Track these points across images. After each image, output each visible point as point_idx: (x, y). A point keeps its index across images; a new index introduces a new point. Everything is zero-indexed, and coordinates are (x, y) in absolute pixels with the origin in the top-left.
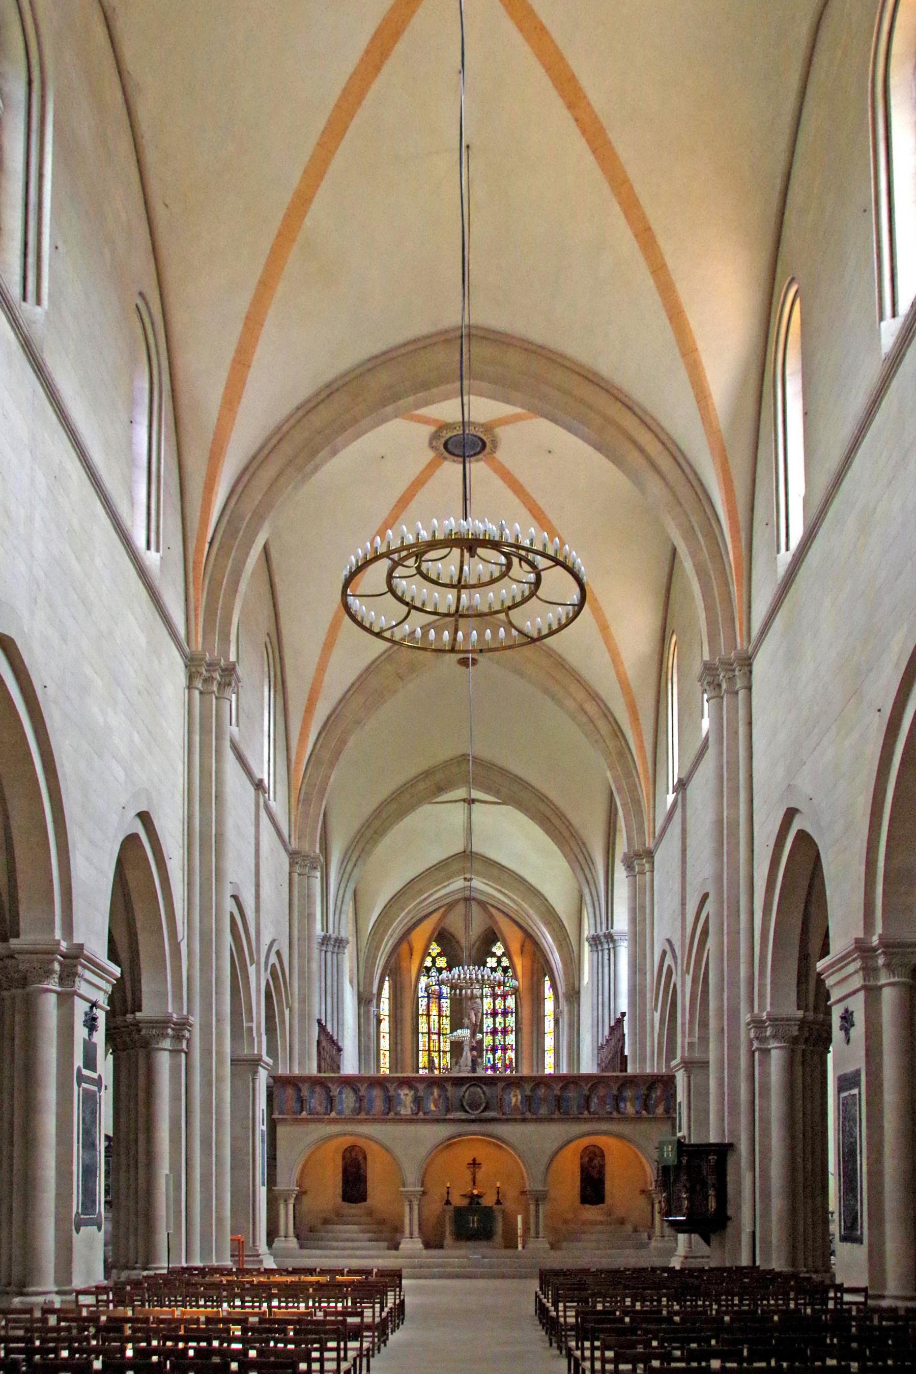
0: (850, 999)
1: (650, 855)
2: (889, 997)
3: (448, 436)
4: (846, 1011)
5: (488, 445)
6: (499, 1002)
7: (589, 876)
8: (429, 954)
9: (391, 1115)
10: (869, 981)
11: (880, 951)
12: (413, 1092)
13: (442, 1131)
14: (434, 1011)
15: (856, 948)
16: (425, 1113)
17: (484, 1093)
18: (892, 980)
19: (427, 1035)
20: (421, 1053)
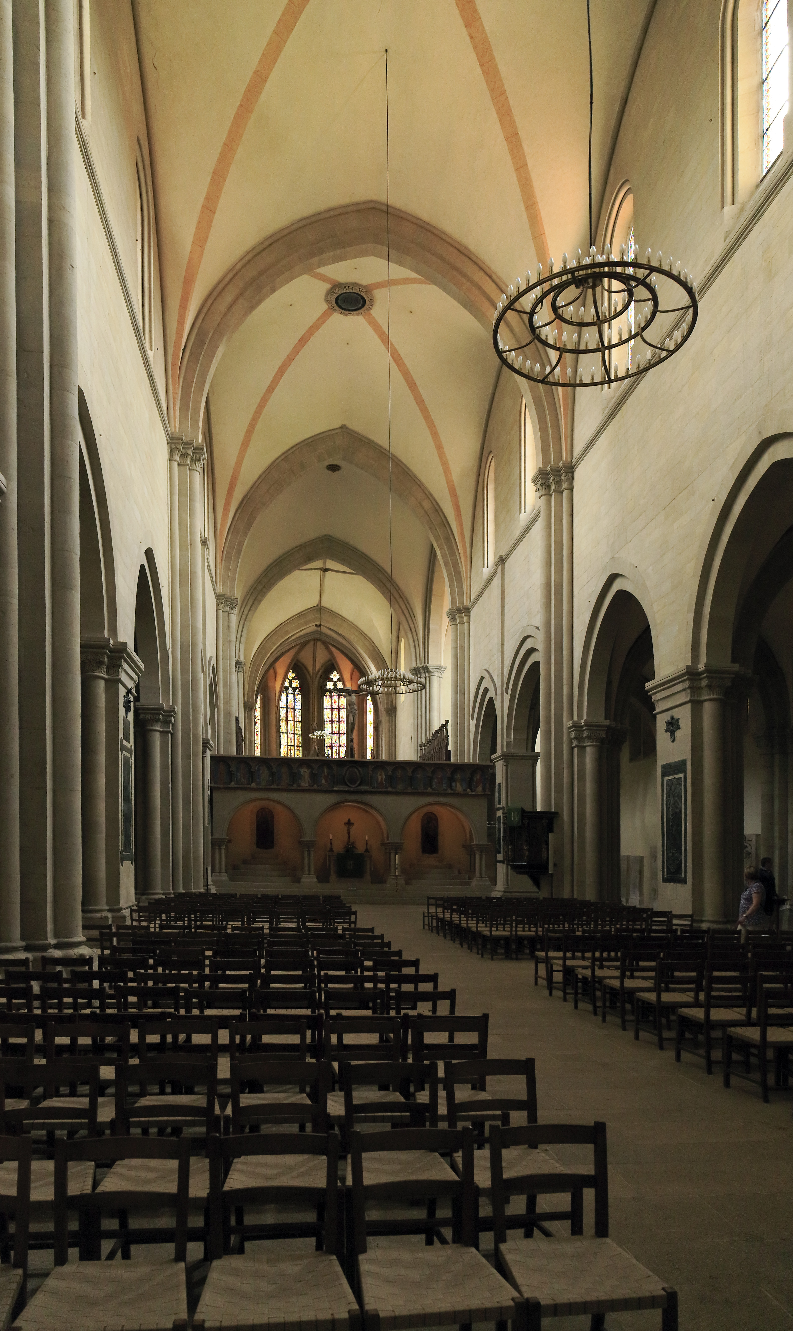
0: (675, 710)
1: (467, 610)
2: (708, 709)
3: (340, 293)
4: (672, 718)
5: (368, 302)
6: (335, 713)
7: (412, 626)
8: (288, 679)
9: (295, 787)
10: (694, 696)
11: (705, 675)
12: (310, 770)
13: (330, 799)
14: (291, 718)
15: (687, 672)
16: (318, 786)
17: (359, 771)
18: (712, 697)
19: (286, 734)
20: (282, 747)
